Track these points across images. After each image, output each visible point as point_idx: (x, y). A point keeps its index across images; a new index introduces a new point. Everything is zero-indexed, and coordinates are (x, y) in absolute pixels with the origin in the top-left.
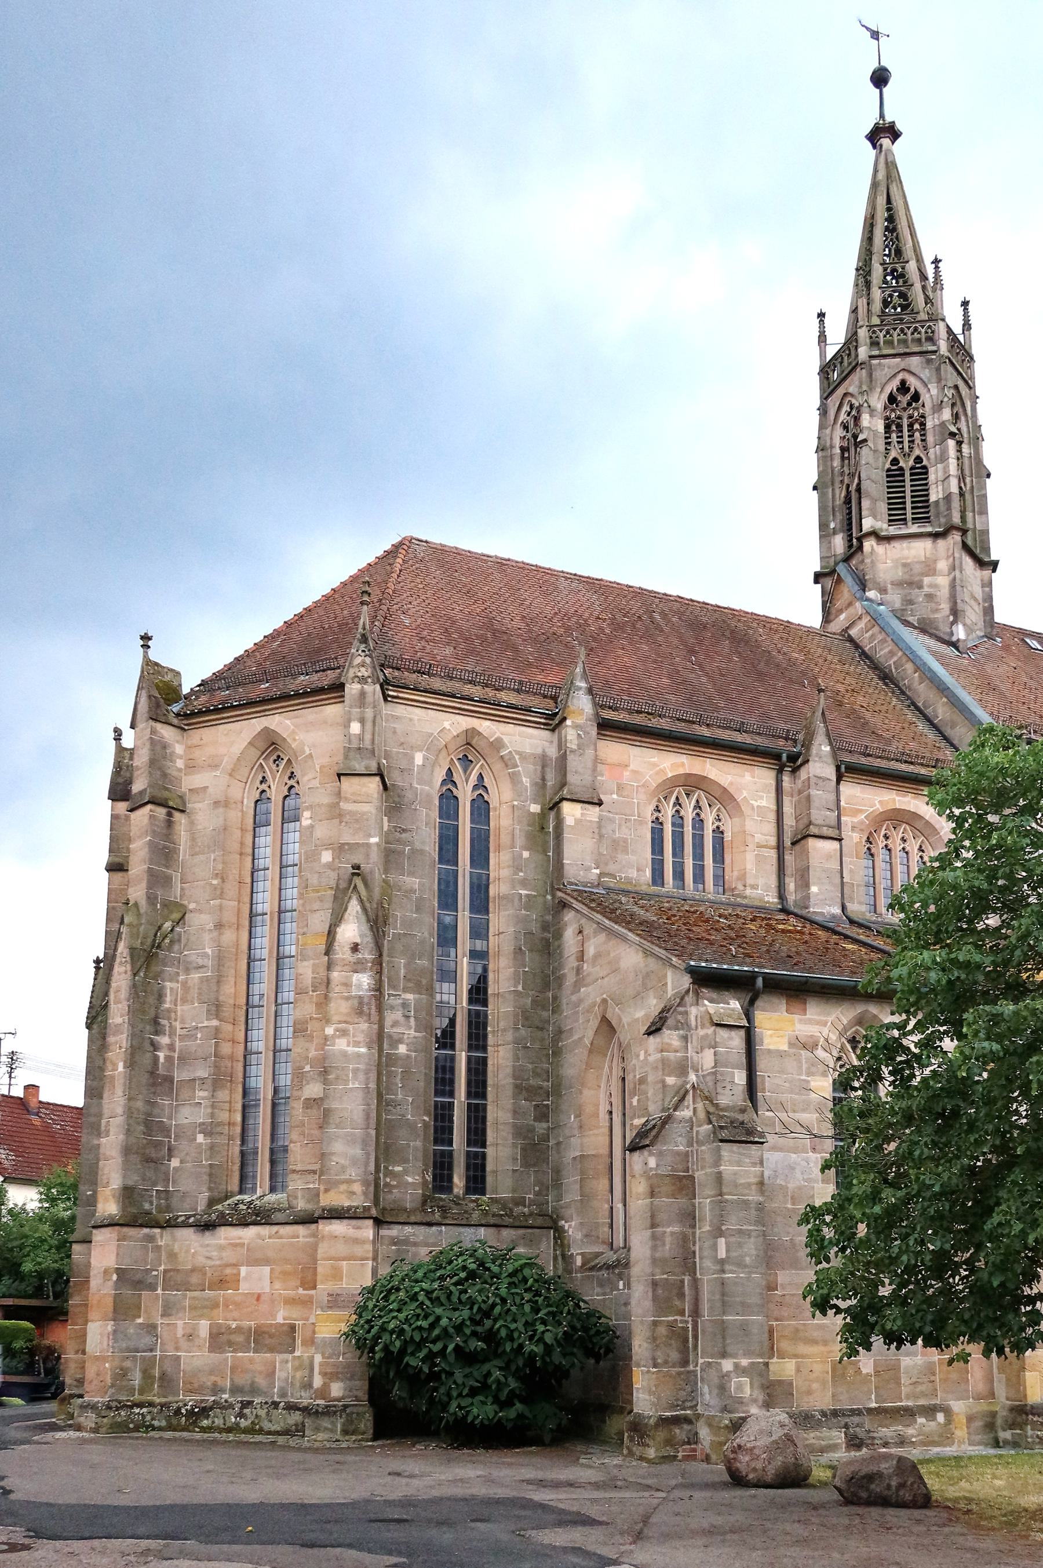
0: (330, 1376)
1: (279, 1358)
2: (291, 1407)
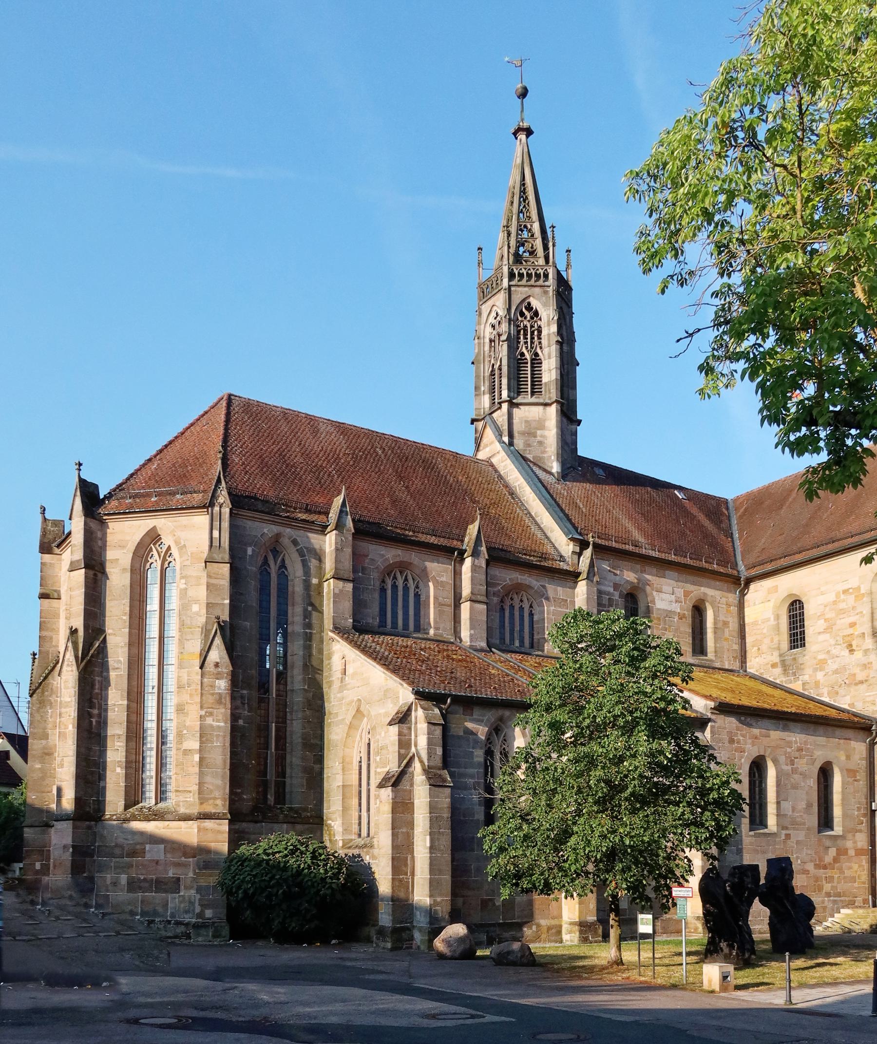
0: (204, 906)
1: (170, 896)
2: (178, 923)
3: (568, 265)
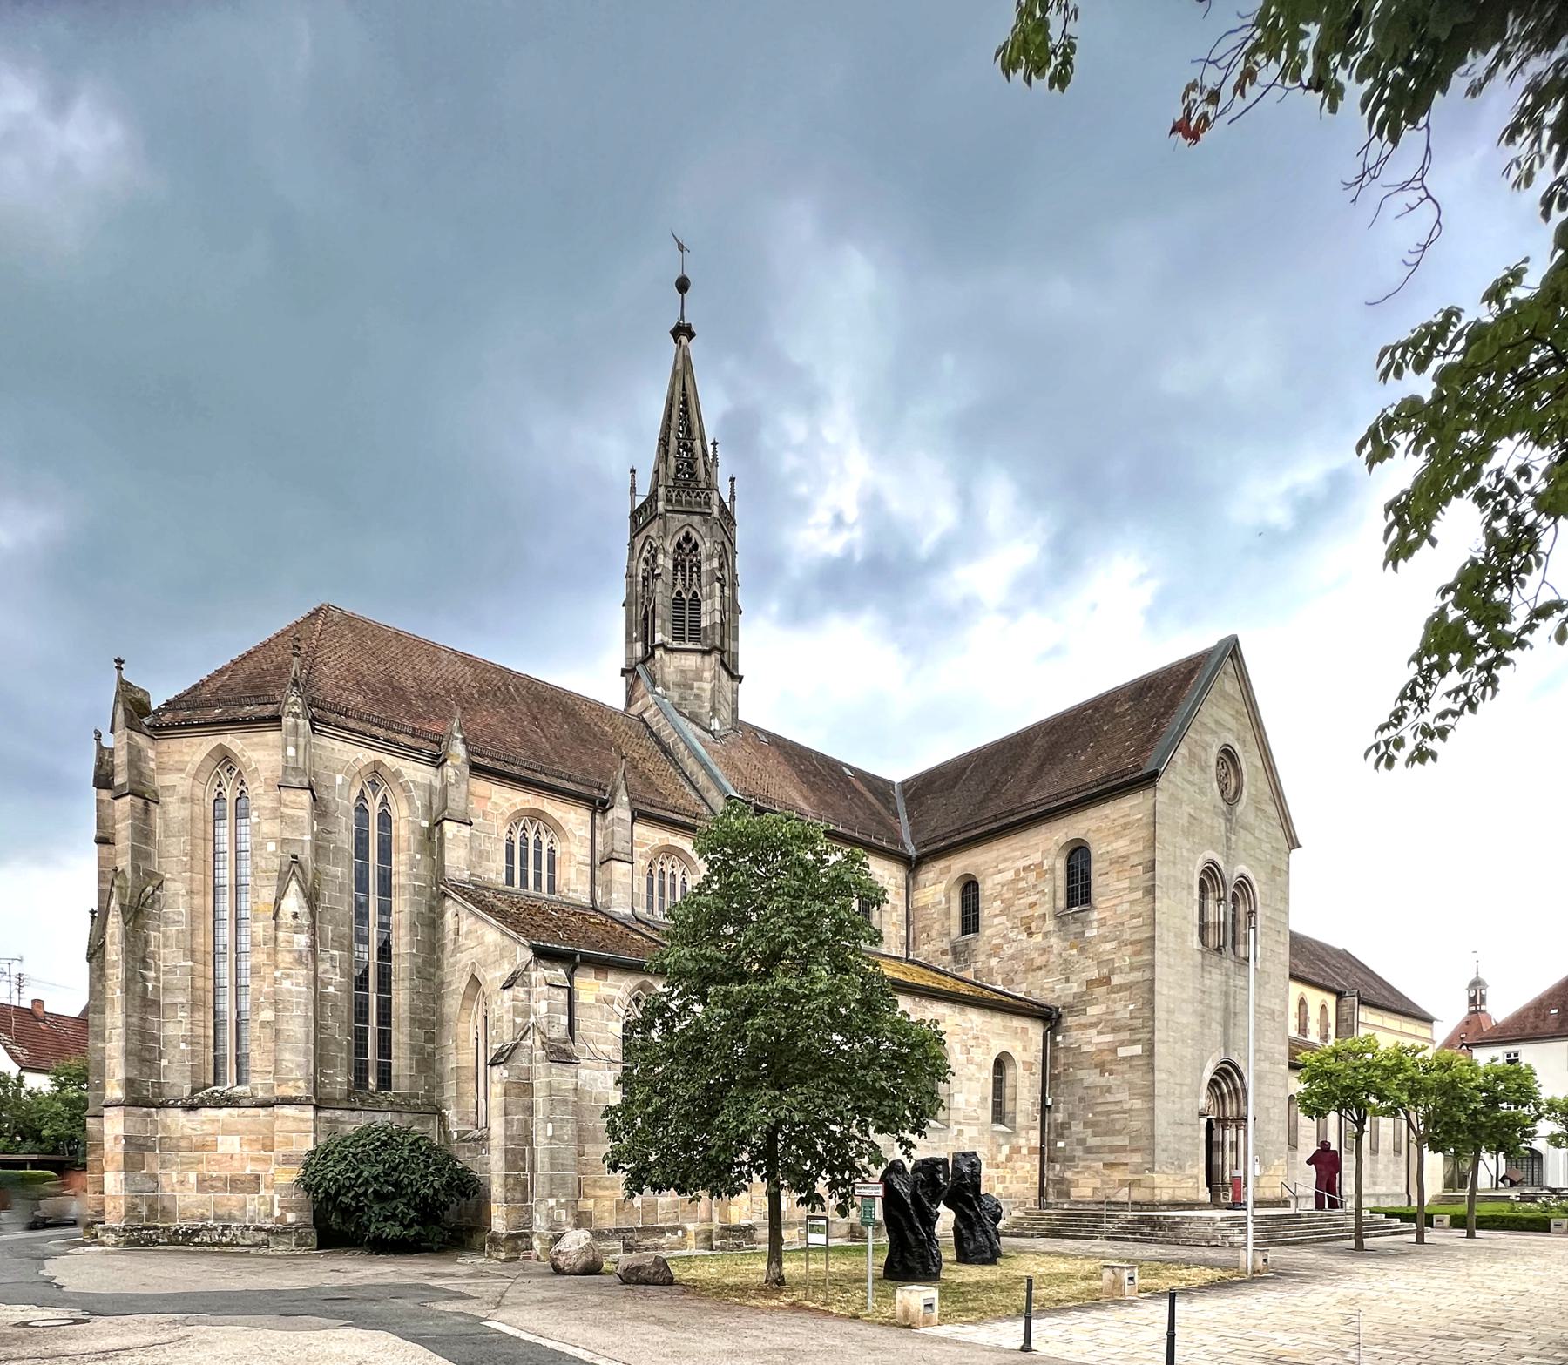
0: (286, 1209)
1: (248, 1197)
2: (258, 1229)
3: (733, 497)
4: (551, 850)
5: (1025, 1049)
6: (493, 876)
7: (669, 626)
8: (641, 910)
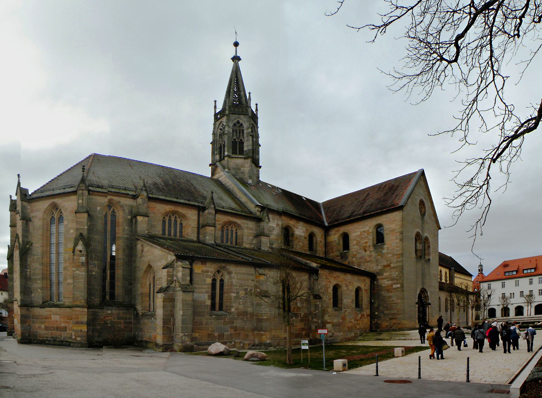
4: (181, 224)
5: (365, 285)
6: (157, 233)
7: (231, 150)
8: (218, 242)
